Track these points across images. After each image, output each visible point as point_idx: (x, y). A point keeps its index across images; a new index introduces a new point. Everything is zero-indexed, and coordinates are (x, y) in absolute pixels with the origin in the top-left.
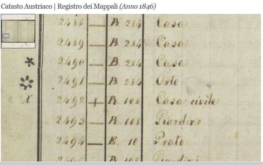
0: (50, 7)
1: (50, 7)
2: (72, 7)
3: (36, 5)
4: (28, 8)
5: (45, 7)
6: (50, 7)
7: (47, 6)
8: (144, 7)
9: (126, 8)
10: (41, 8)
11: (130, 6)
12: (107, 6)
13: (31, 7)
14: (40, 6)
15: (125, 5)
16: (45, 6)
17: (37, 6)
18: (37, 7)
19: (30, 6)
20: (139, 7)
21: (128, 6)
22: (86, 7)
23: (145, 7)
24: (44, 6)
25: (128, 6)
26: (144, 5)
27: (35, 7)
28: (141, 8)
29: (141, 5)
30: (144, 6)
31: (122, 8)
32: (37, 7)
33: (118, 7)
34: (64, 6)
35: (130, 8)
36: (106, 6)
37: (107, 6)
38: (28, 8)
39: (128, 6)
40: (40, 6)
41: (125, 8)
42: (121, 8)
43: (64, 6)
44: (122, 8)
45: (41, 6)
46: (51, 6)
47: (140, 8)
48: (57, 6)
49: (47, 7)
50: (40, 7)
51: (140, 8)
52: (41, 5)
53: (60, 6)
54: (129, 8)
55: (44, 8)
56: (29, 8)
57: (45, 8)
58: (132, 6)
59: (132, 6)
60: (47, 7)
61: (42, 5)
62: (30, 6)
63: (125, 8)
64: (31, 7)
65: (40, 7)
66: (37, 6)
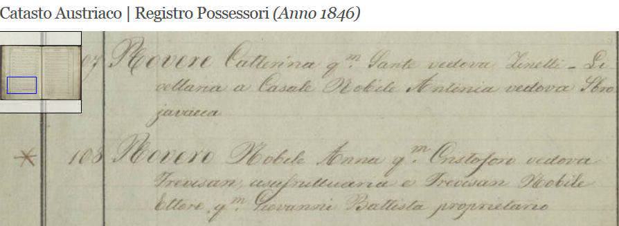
0: (116, 14)
1: (116, 14)
3: (84, 11)
4: (64, 18)
5: (105, 15)
6: (118, 14)
7: (110, 12)
8: (332, 15)
9: (289, 15)
10: (96, 18)
12: (259, 13)
14: (93, 11)
15: (285, 9)
16: (104, 13)
17: (87, 13)
18: (87, 16)
19: (68, 11)
20: (320, 14)
22: (261, 15)
23: (335, 15)
24: (102, 12)
25: (294, 13)
26: (333, 10)
27: (82, 14)
28: (326, 16)
29: (325, 11)
30: (331, 12)
31: (279, 18)
32: (87, 16)
33: (271, 15)
34: (233, 13)
35: (298, 16)
37: (259, 13)
38: (64, 18)
39: (294, 13)
40: (93, 11)
41: (287, 18)
42: (277, 16)
44: (279, 18)
45: (267, 11)
46: (192, 13)
47: (323, 18)
48: (133, 13)
49: (111, 15)
50: (93, 15)
52: (95, 9)
53: (140, 12)
54: (296, 18)
55: (102, 16)
56: (66, 16)
57: (104, 18)
58: (304, 13)
59: (304, 13)
60: (111, 15)
61: (98, 10)
62: (68, 11)
63: (287, 18)
65: (93, 15)
66: (87, 13)
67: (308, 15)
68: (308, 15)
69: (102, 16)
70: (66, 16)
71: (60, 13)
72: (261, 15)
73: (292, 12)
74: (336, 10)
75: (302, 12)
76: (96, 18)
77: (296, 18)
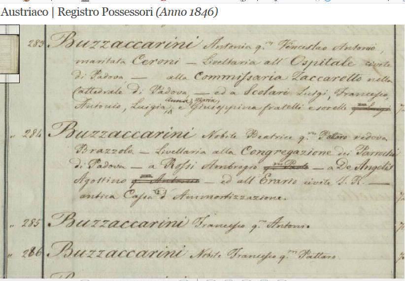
2: (123, 13)
3: (21, 10)
8: (198, 13)
9: (167, 14)
10: (30, 15)
11: (175, 11)
12: (146, 12)
13: (12, 14)
14: (28, 11)
15: (165, 9)
17: (23, 12)
18: (23, 14)
19: (10, 11)
20: (189, 13)
21: (170, 11)
22: (147, 13)
23: (200, 13)
24: (34, 11)
25: (171, 12)
26: (198, 10)
27: (20, 12)
28: (194, 14)
29: (192, 10)
31: (160, 15)
32: (23, 14)
34: (127, 11)
36: (209, 14)
37: (146, 12)
38: (7, 15)
40: (28, 11)
41: (166, 15)
42: (158, 14)
43: (127, 11)
44: (160, 15)
47: (192, 15)
48: (56, 11)
49: (40, 13)
50: (28, 13)
51: (192, 15)
52: (30, 9)
53: (61, 12)
54: (172, 15)
55: (34, 14)
56: (9, 14)
57: (36, 15)
58: (178, 12)
59: (178, 12)
60: (40, 13)
62: (10, 11)
63: (166, 15)
64: (12, 14)
65: (28, 13)
66: (23, 12)
67: (181, 13)
68: (181, 13)
69: (34, 14)
70: (9, 14)
71: (5, 11)
72: (147, 13)
73: (170, 11)
74: (201, 9)
75: (176, 11)
76: (30, 15)
77: (172, 15)
